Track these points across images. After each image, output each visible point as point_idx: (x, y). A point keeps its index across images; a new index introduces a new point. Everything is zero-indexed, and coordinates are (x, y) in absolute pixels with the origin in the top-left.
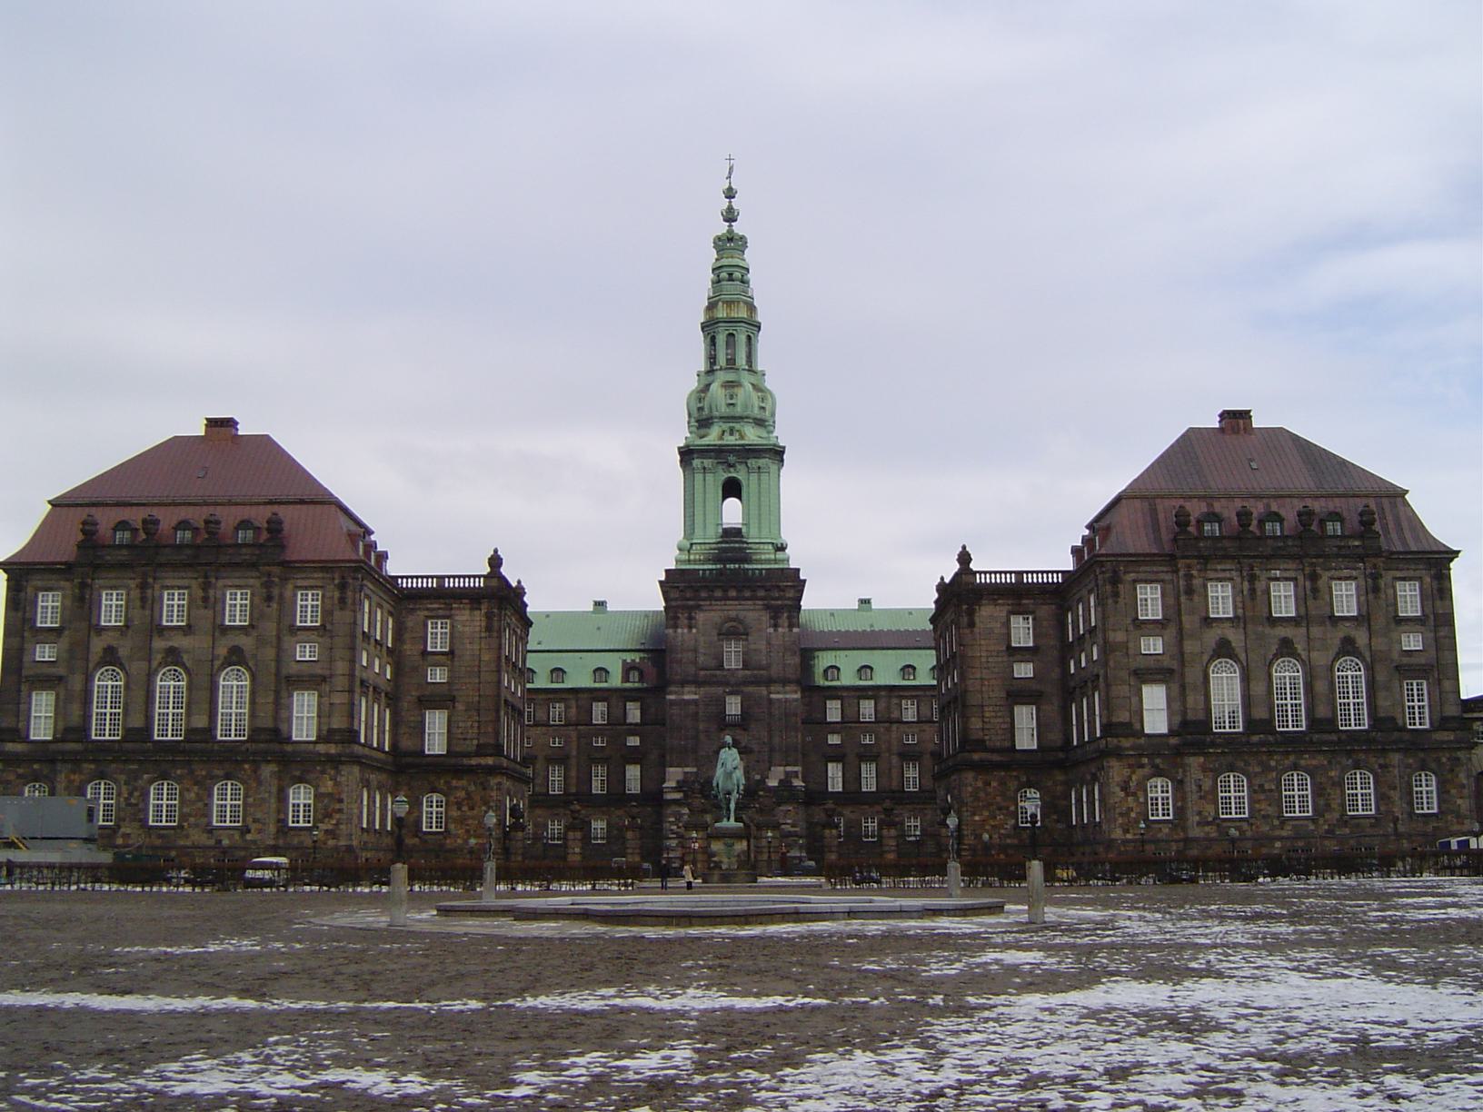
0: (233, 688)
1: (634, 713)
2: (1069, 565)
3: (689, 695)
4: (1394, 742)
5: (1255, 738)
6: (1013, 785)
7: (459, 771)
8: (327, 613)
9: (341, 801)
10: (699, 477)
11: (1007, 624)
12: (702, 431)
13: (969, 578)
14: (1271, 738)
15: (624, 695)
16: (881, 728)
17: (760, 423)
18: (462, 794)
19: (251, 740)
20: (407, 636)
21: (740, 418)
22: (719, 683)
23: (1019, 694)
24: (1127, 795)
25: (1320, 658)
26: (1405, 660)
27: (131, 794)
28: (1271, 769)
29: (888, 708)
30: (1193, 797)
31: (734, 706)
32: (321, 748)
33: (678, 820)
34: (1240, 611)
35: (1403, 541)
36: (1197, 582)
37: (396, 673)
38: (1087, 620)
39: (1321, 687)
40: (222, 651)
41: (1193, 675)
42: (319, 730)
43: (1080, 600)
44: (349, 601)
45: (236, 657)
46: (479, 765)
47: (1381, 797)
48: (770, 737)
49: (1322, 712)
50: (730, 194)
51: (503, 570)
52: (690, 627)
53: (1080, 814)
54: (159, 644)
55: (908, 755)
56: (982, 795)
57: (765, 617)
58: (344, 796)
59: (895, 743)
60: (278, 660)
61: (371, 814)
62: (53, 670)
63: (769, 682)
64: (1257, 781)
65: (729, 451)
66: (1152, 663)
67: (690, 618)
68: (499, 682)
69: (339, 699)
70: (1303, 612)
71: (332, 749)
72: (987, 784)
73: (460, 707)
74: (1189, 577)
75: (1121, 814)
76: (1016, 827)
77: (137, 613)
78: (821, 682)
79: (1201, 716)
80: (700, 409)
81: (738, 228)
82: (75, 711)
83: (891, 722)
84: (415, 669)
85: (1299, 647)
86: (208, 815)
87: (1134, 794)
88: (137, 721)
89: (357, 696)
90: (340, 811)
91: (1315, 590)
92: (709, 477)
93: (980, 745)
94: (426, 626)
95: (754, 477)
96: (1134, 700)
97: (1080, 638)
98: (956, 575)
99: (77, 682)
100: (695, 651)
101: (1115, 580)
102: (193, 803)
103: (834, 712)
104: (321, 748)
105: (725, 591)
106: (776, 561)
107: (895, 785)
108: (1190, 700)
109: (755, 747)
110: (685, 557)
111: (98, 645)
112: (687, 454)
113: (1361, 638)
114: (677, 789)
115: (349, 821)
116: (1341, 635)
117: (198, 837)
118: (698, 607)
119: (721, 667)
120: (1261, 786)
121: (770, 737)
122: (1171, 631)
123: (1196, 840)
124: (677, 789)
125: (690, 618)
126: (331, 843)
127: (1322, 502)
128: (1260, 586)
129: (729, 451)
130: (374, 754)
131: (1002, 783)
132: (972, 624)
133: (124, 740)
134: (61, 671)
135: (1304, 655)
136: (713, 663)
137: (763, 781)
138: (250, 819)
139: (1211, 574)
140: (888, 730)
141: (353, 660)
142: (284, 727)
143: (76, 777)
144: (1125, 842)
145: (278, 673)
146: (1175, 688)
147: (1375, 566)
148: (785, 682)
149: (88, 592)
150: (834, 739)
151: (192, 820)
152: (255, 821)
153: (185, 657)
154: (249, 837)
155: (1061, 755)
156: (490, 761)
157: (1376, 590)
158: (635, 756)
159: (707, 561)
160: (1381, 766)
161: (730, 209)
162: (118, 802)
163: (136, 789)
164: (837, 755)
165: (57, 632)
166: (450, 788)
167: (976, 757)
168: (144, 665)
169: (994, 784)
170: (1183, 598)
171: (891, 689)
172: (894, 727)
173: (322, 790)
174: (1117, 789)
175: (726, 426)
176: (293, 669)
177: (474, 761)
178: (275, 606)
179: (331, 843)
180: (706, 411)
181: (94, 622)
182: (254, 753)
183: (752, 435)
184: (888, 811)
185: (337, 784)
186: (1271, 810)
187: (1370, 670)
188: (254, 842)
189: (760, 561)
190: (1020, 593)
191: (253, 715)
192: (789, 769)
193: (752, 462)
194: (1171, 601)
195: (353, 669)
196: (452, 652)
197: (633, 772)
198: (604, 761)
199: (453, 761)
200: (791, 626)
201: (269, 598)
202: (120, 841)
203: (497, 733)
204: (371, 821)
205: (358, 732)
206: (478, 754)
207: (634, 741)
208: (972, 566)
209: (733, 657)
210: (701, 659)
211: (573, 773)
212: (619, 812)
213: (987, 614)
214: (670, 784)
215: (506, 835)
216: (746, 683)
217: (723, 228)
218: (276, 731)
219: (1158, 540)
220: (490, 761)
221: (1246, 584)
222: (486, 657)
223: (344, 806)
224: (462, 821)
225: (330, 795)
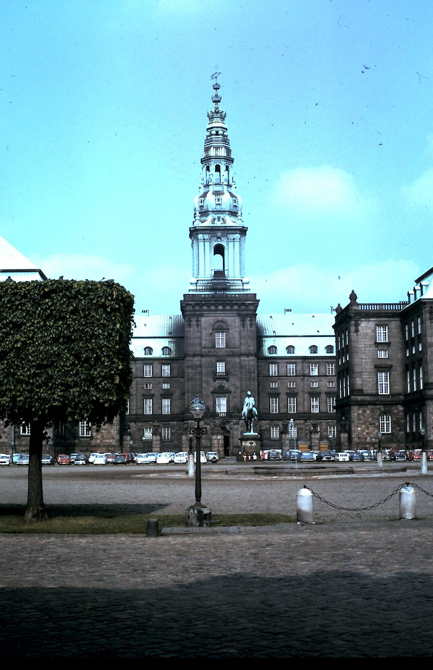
1: (166, 370)
10: (201, 244)
11: (375, 331)
12: (203, 218)
13: (355, 308)
15: (162, 361)
16: (299, 379)
17: (234, 214)
21: (224, 211)
23: (380, 367)
31: (221, 368)
38: (416, 330)
43: (412, 320)
50: (216, 88)
56: (362, 417)
59: (306, 387)
63: (240, 355)
67: (198, 321)
72: (365, 412)
78: (266, 353)
80: (201, 207)
81: (222, 107)
83: (304, 376)
92: (207, 244)
93: (361, 392)
95: (231, 244)
97: (412, 339)
103: (273, 369)
105: (216, 306)
106: (243, 290)
107: (306, 410)
109: (232, 389)
110: (194, 287)
112: (194, 232)
118: (202, 315)
125: (198, 321)
131: (372, 411)
132: (357, 331)
136: (210, 345)
148: (248, 355)
158: (166, 395)
159: (205, 290)
161: (216, 96)
169: (368, 412)
171: (305, 358)
175: (216, 216)
180: (205, 208)
183: (230, 222)
189: (235, 290)
190: (381, 314)
193: (231, 236)
207: (166, 386)
208: (357, 301)
209: (221, 341)
210: (204, 342)
213: (366, 326)
216: (228, 356)
217: (212, 107)
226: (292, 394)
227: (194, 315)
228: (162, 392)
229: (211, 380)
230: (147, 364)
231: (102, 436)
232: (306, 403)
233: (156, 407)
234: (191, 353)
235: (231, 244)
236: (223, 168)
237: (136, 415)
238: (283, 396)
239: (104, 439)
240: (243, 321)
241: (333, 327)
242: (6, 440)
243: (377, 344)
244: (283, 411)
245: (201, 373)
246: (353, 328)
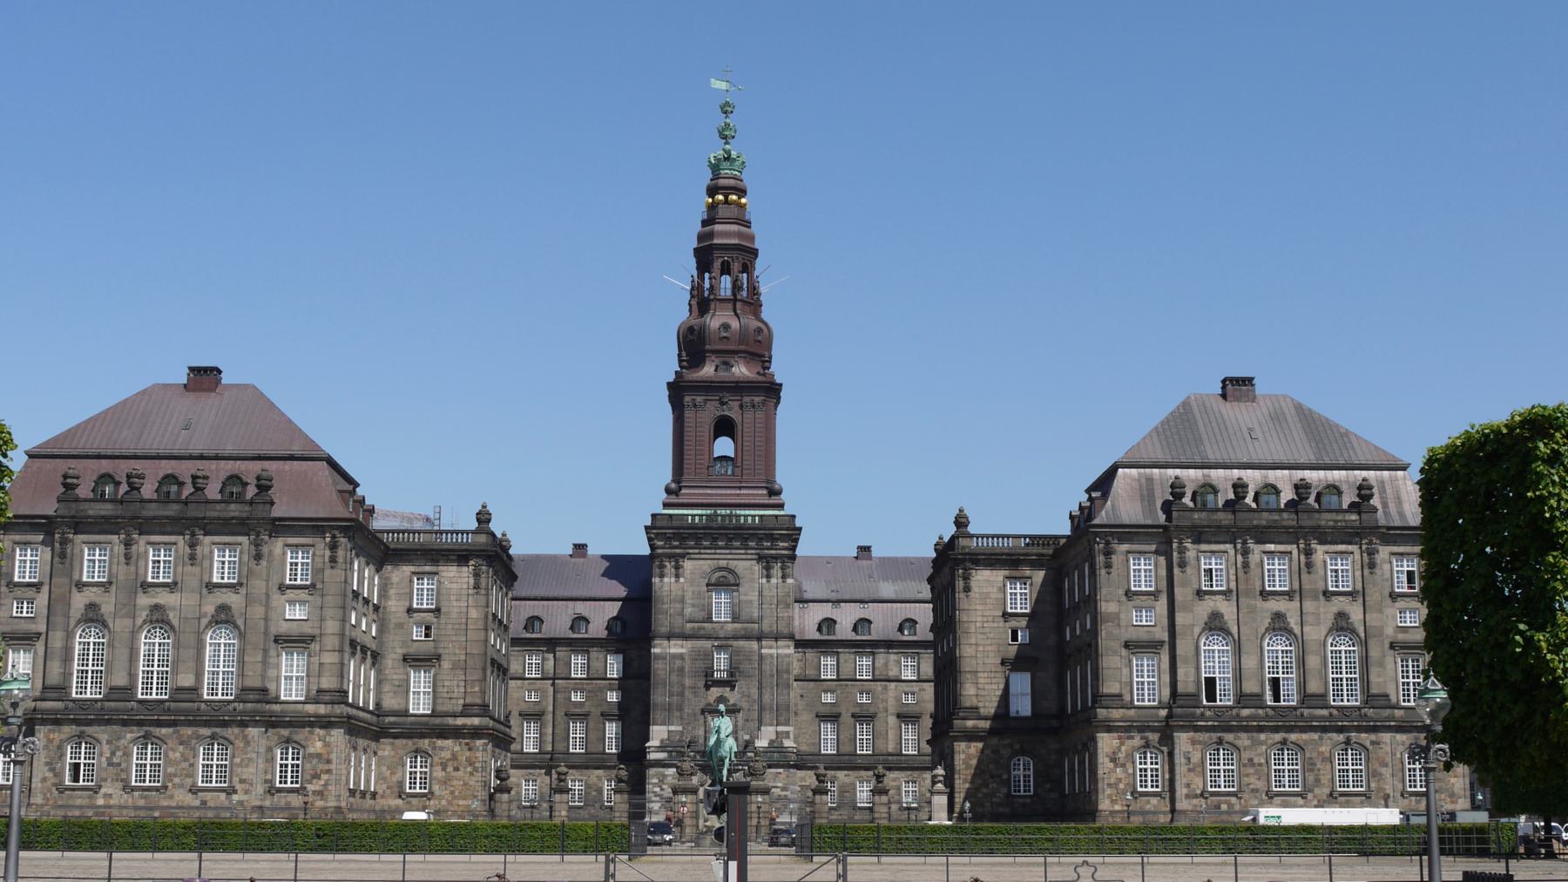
0: (219, 647)
2: (1064, 528)
3: (676, 648)
4: (1388, 719)
5: (1245, 712)
6: (1005, 752)
7: (444, 733)
8: (318, 572)
9: (329, 761)
14: (1260, 711)
16: (879, 686)
18: (446, 755)
19: (238, 699)
20: (392, 592)
22: (708, 638)
24: (1116, 766)
25: (1314, 633)
26: (1401, 637)
27: (113, 754)
28: (1261, 743)
29: (886, 664)
30: (1181, 769)
31: (721, 661)
32: (310, 708)
33: (661, 781)
34: (1233, 585)
35: (1401, 514)
36: (1191, 554)
37: (380, 631)
38: (1082, 588)
39: (1313, 661)
40: (210, 609)
41: (1182, 647)
42: (308, 690)
43: (1076, 567)
44: (340, 560)
45: (223, 617)
46: (464, 726)
47: (1373, 774)
48: (761, 695)
49: (1314, 687)
51: (493, 526)
52: (677, 576)
53: (1072, 783)
54: (144, 601)
55: (906, 717)
57: (757, 568)
58: (333, 756)
60: (266, 619)
61: (357, 776)
62: (33, 628)
64: (1246, 755)
65: (722, 384)
66: (1142, 635)
67: (677, 567)
68: (486, 641)
69: (330, 658)
70: (1296, 586)
71: (322, 709)
73: (446, 665)
74: (1182, 551)
75: (1109, 785)
76: (1008, 795)
77: (122, 571)
79: (1191, 689)
82: (55, 669)
84: (400, 626)
85: (1293, 622)
86: (192, 775)
87: (1123, 765)
88: (120, 680)
89: (347, 656)
90: (329, 771)
91: (1309, 565)
94: (411, 581)
96: (1125, 671)
97: (1076, 607)
98: (953, 538)
99: (57, 640)
100: (682, 601)
101: (1108, 553)
102: (175, 763)
104: (310, 708)
105: (715, 539)
108: (1181, 672)
109: (745, 705)
111: (79, 601)
112: (677, 391)
113: (1356, 613)
114: (661, 748)
115: (338, 782)
116: (1335, 609)
117: (182, 797)
118: (683, 556)
119: (709, 619)
120: (1251, 760)
121: (761, 695)
122: (1163, 600)
123: (1184, 812)
124: (661, 748)
125: (677, 567)
126: (320, 803)
127: (1321, 473)
128: (1254, 558)
129: (722, 384)
130: (361, 714)
132: (967, 589)
133: (106, 699)
134: (42, 628)
135: (1297, 630)
137: (748, 745)
138: (236, 780)
139: (1204, 547)
140: (885, 688)
141: (344, 620)
142: (272, 687)
143: (56, 737)
144: (1113, 813)
145: (266, 633)
146: (1165, 658)
147: (1370, 543)
149: (69, 547)
150: (828, 698)
151: (177, 780)
152: (242, 781)
153: (171, 615)
154: (235, 797)
155: (1055, 723)
156: (476, 721)
157: (1372, 565)
160: (1373, 743)
162: (100, 762)
163: (118, 748)
164: (832, 717)
165: (37, 586)
166: (434, 748)
167: (970, 723)
168: (128, 622)
170: (1176, 570)
172: (893, 685)
173: (311, 750)
174: (1107, 760)
176: (284, 628)
177: (460, 721)
178: (264, 563)
179: (320, 803)
181: (76, 577)
182: (242, 713)
184: (879, 778)
185: (327, 745)
186: (1260, 784)
187: (1365, 644)
188: (241, 803)
191: (242, 674)
192: (780, 729)
194: (1163, 572)
195: (343, 628)
196: (437, 610)
197: (612, 729)
198: (583, 717)
199: (438, 721)
200: (784, 577)
201: (258, 557)
202: (100, 802)
203: (483, 692)
204: (357, 783)
205: (346, 692)
206: (462, 715)
210: (688, 611)
211: (550, 730)
212: (600, 772)
213: (985, 580)
214: (653, 742)
215: (491, 797)
216: (736, 638)
218: (264, 690)
219: (1152, 511)
220: (476, 721)
221: (1240, 558)
222: (474, 614)
223: (333, 767)
224: (445, 782)
225: (319, 756)
226: (865, 717)
227: (670, 556)
228: (605, 708)
229: (701, 684)
230: (576, 652)
231: (452, 793)
232: (892, 735)
233: (592, 736)
234: (664, 630)
235: (749, 415)
236: (736, 267)
237: (552, 753)
238: (846, 718)
239: (455, 798)
240: (768, 568)
241: (930, 580)
242: (245, 798)
243: (1006, 616)
244: (846, 749)
245: (681, 670)
246: (960, 584)
